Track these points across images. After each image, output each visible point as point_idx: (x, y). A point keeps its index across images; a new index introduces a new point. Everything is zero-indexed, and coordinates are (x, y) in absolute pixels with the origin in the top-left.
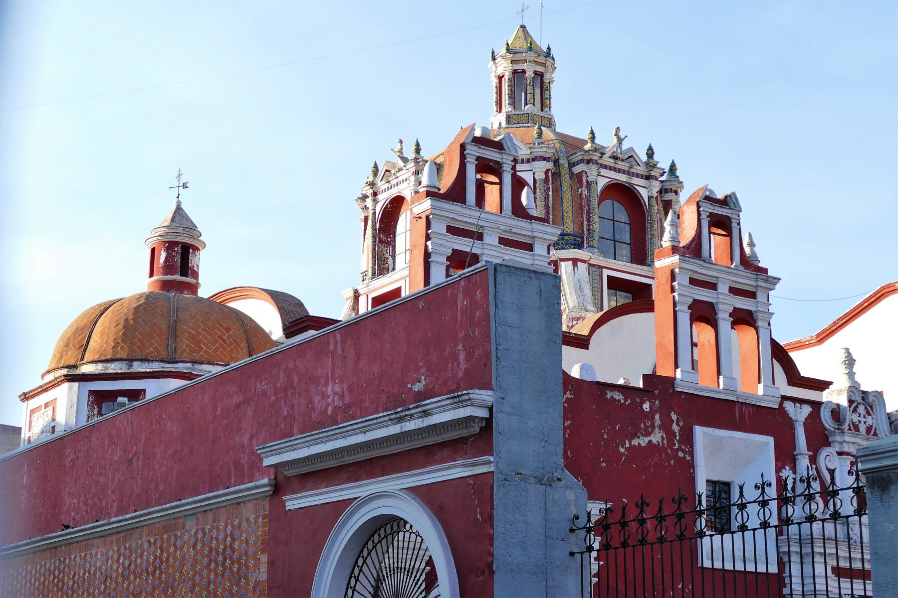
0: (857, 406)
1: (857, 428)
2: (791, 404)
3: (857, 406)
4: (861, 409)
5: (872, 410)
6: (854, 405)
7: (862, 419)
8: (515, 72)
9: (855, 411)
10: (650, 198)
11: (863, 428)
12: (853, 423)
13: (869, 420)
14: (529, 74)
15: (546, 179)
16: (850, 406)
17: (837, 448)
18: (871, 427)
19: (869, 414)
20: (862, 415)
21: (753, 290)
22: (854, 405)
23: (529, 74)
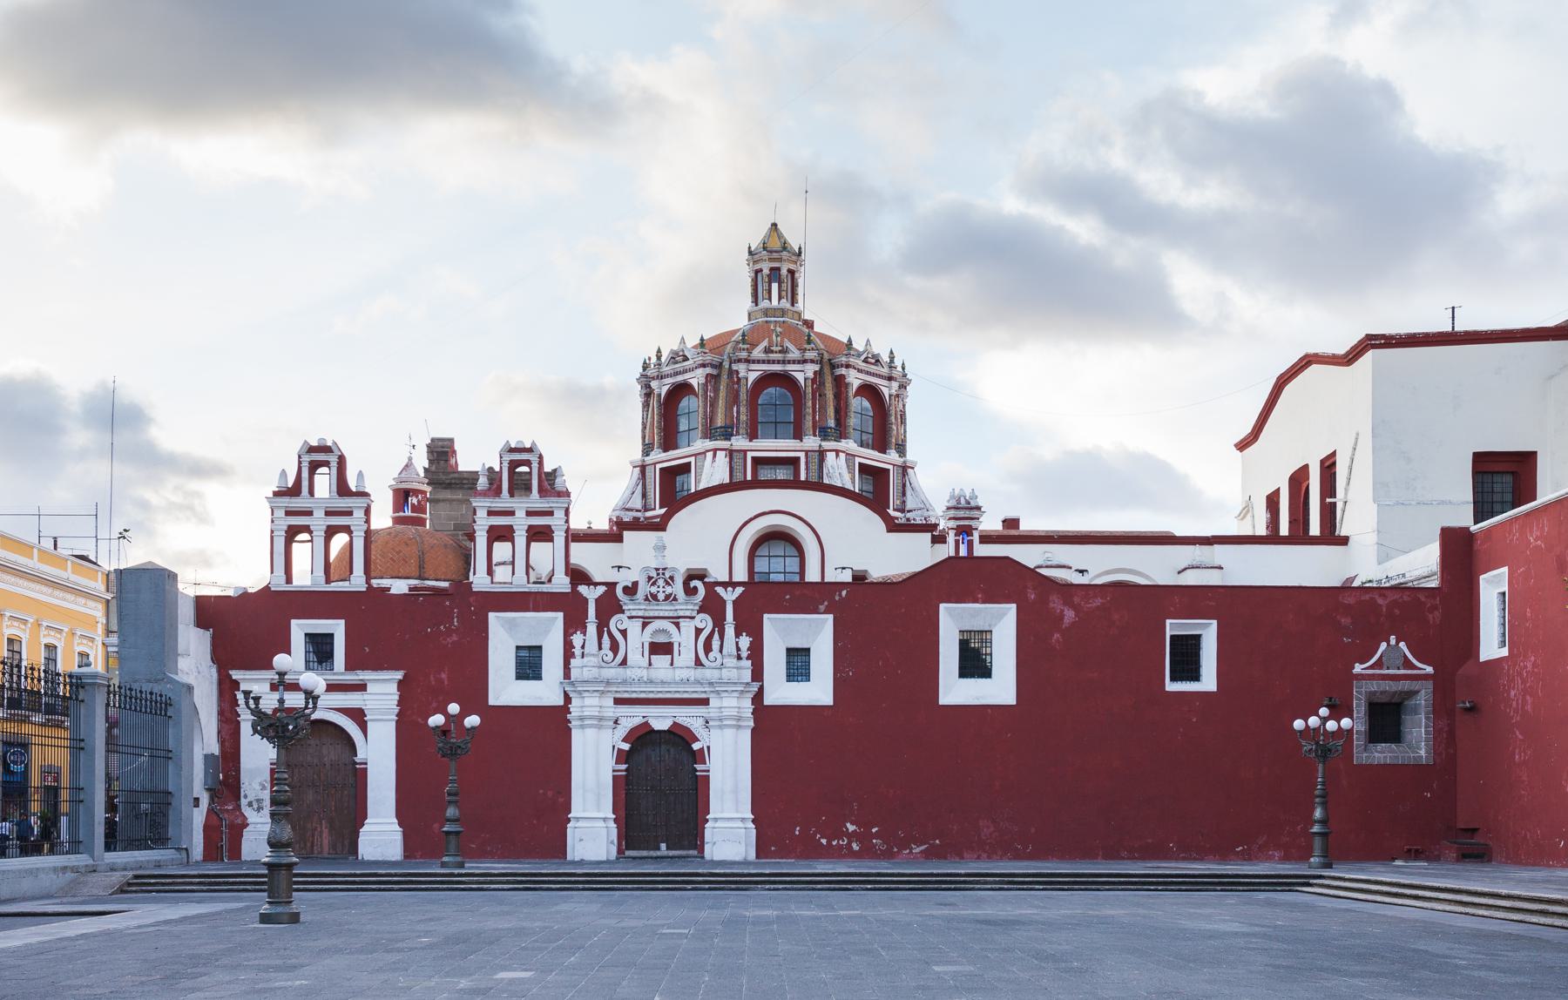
0: (656, 580)
1: (655, 597)
3: (656, 580)
4: (661, 582)
5: (673, 582)
6: (653, 580)
7: (661, 589)
8: (772, 269)
9: (654, 584)
10: (805, 379)
11: (661, 596)
12: (651, 594)
13: (669, 590)
15: (706, 385)
16: (649, 582)
17: (628, 613)
19: (670, 585)
20: (661, 587)
21: (551, 510)
22: (653, 580)
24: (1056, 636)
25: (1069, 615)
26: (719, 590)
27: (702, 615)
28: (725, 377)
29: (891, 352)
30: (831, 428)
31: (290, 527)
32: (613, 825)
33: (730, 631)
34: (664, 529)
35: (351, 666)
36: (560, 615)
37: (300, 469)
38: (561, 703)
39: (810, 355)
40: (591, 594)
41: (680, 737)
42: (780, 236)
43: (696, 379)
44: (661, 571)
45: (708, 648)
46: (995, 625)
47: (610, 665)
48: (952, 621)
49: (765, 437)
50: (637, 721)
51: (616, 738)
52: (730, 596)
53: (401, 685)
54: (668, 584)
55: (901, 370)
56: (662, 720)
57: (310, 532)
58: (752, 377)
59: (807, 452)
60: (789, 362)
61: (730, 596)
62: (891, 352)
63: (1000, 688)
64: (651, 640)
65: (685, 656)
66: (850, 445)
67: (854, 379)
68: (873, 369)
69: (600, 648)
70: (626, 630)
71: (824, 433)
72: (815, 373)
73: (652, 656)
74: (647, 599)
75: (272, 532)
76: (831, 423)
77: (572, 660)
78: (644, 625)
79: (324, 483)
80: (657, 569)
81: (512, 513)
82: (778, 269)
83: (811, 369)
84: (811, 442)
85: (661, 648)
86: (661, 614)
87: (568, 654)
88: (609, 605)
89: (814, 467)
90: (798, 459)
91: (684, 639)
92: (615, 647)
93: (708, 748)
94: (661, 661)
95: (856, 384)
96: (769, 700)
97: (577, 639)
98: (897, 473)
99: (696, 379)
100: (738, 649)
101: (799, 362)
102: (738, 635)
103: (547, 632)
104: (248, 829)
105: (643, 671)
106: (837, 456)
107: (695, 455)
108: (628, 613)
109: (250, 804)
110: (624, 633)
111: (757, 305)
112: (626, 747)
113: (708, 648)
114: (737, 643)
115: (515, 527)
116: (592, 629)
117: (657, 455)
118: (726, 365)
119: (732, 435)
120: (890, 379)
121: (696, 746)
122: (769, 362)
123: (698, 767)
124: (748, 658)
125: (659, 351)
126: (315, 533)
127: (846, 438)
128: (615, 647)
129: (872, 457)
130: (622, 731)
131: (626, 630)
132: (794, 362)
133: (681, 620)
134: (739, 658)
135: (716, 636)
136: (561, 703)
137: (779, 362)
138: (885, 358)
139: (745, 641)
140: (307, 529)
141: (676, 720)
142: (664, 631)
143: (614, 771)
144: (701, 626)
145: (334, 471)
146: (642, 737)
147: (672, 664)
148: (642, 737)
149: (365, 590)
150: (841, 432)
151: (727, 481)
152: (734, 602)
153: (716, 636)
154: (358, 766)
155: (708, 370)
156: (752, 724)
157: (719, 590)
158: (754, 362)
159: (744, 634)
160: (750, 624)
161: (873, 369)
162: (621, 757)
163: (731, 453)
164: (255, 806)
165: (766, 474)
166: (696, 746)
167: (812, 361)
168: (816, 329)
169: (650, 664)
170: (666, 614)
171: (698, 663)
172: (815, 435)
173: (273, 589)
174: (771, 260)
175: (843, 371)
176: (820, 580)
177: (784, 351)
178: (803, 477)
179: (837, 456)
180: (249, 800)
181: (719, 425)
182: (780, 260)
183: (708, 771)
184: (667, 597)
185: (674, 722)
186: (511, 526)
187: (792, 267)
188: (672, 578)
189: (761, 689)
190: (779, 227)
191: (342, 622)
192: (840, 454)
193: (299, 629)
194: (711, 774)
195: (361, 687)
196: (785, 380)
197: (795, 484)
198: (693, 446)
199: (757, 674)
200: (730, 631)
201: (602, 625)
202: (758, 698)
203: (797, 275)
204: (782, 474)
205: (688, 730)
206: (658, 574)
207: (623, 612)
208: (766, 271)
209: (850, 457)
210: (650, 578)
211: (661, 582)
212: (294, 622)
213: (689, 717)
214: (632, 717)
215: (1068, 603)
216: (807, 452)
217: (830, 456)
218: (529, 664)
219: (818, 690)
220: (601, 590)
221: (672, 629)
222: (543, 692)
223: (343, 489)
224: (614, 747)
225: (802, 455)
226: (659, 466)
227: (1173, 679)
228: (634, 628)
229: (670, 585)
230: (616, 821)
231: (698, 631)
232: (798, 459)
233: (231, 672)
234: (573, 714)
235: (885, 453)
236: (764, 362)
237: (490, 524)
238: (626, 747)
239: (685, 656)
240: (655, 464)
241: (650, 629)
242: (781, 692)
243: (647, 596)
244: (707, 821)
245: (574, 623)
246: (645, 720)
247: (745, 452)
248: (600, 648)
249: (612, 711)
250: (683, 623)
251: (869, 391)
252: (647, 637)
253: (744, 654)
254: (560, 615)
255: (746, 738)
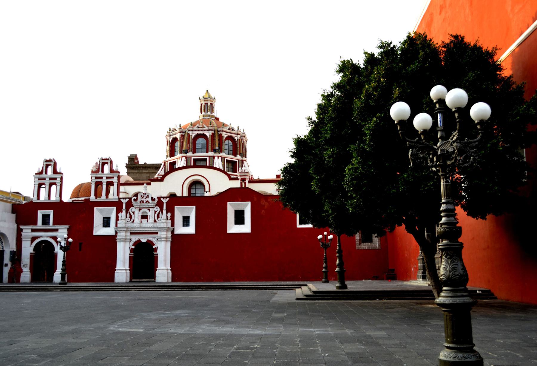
1: (143, 202)
2: (123, 199)
4: (145, 197)
7: (145, 199)
9: (143, 198)
11: (145, 201)
13: (147, 199)
14: (209, 104)
17: (135, 207)
18: (148, 201)
23: (209, 104)
24: (263, 211)
25: (267, 204)
26: (162, 199)
27: (156, 207)
28: (186, 135)
29: (238, 127)
30: (217, 150)
31: (39, 183)
32: (128, 271)
33: (164, 212)
34: (163, 181)
35: (54, 224)
36: (115, 208)
37: (43, 166)
38: (114, 234)
39: (210, 128)
40: (124, 201)
41: (150, 244)
42: (209, 94)
43: (178, 136)
44: (145, 194)
45: (158, 217)
46: (245, 208)
47: (129, 223)
48: (231, 208)
49: (198, 153)
50: (137, 239)
51: (130, 245)
52: (165, 201)
53: (68, 229)
54: (147, 198)
55: (243, 132)
56: (144, 239)
57: (45, 185)
58: (194, 135)
59: (209, 157)
60: (204, 130)
61: (165, 201)
62: (238, 127)
63: (246, 228)
64: (141, 215)
65: (151, 219)
66: (223, 154)
67: (225, 135)
68: (232, 132)
69: (126, 217)
70: (134, 212)
71: (215, 151)
72: (212, 133)
73: (142, 220)
74: (141, 202)
75: (34, 185)
76: (217, 148)
77: (118, 221)
78: (140, 210)
79: (50, 170)
80: (144, 193)
81: (102, 178)
82: (207, 103)
83: (211, 133)
84: (211, 154)
85: (144, 217)
86: (145, 207)
87: (117, 219)
88: (129, 205)
89: (211, 161)
90: (207, 159)
91: (151, 214)
92: (131, 217)
93: (158, 247)
94: (144, 221)
95: (225, 136)
96: (176, 232)
97: (120, 215)
98: (240, 163)
99: (178, 136)
100: (167, 217)
101: (207, 130)
102: (167, 213)
103: (111, 213)
104: (23, 273)
105: (137, 224)
106: (218, 158)
107: (177, 158)
108: (135, 207)
109: (24, 266)
110: (134, 213)
111: (201, 113)
112: (133, 247)
113: (158, 217)
114: (167, 215)
115: (103, 182)
116: (124, 212)
117: (169, 159)
118: (187, 132)
119: (188, 152)
120: (237, 134)
121: (154, 247)
122: (199, 131)
123: (155, 253)
124: (170, 220)
125: (170, 128)
126: (46, 185)
127: (222, 152)
128: (131, 217)
129: (232, 158)
130: (132, 243)
131: (134, 212)
132: (206, 130)
133: (150, 208)
134: (167, 219)
135: (161, 213)
136: (114, 234)
137: (201, 131)
138: (236, 129)
139: (169, 215)
140: (55, 184)
141: (148, 239)
142: (146, 212)
143: (130, 255)
144: (156, 210)
145: (53, 167)
146: (138, 244)
147: (148, 222)
148: (138, 244)
149: (59, 201)
150: (220, 150)
151: (185, 165)
152: (166, 203)
153: (161, 213)
154: (55, 254)
155: (181, 134)
156: (171, 240)
157: (162, 199)
158: (194, 131)
159: (169, 212)
160: (170, 209)
161: (232, 132)
162: (132, 250)
163: (186, 157)
164: (25, 266)
165: (198, 164)
166: (154, 247)
167: (211, 130)
168: (220, 120)
169: (141, 222)
170: (146, 207)
171: (155, 221)
172: (212, 152)
173: (34, 202)
174: (205, 101)
175: (221, 133)
176: (181, 196)
177: (203, 127)
178: (208, 165)
179: (218, 158)
180: (24, 264)
181: (184, 150)
182: (208, 101)
183: (157, 254)
184: (147, 202)
185: (148, 240)
186: (102, 182)
187: (211, 102)
188: (148, 196)
189: (174, 229)
190: (208, 91)
191: (52, 211)
192: (219, 157)
193: (40, 214)
194: (158, 255)
195: (57, 230)
196: (204, 136)
197: (206, 167)
198: (178, 155)
199: (173, 224)
200: (164, 212)
201: (127, 210)
202: (173, 232)
203: (213, 105)
204: (203, 164)
205: (152, 242)
206: (144, 195)
207: (133, 206)
208: (204, 104)
209: (222, 158)
210: (142, 196)
211: (145, 197)
212: (39, 211)
213: (152, 238)
214: (135, 238)
215: (267, 201)
216: (209, 157)
217: (216, 158)
218: (106, 223)
219: (191, 229)
220: (127, 200)
221: (148, 211)
222: (109, 231)
223: (55, 172)
224: (130, 247)
225: (208, 158)
226: (169, 162)
227: (300, 223)
228: (136, 211)
229: (147, 198)
230: (130, 270)
231: (155, 212)
232: (207, 159)
233: (20, 226)
234: (118, 237)
235: (236, 156)
236: (197, 131)
237: (96, 181)
238: (133, 247)
239: (151, 219)
240: (168, 161)
241: (141, 211)
242: (181, 230)
243: (141, 201)
244: (157, 270)
245: (119, 210)
246: (139, 239)
247: (191, 157)
248: (126, 217)
249: (129, 236)
250: (151, 209)
251: (230, 138)
252: (140, 214)
253: (169, 218)
254: (115, 208)
255: (169, 244)
